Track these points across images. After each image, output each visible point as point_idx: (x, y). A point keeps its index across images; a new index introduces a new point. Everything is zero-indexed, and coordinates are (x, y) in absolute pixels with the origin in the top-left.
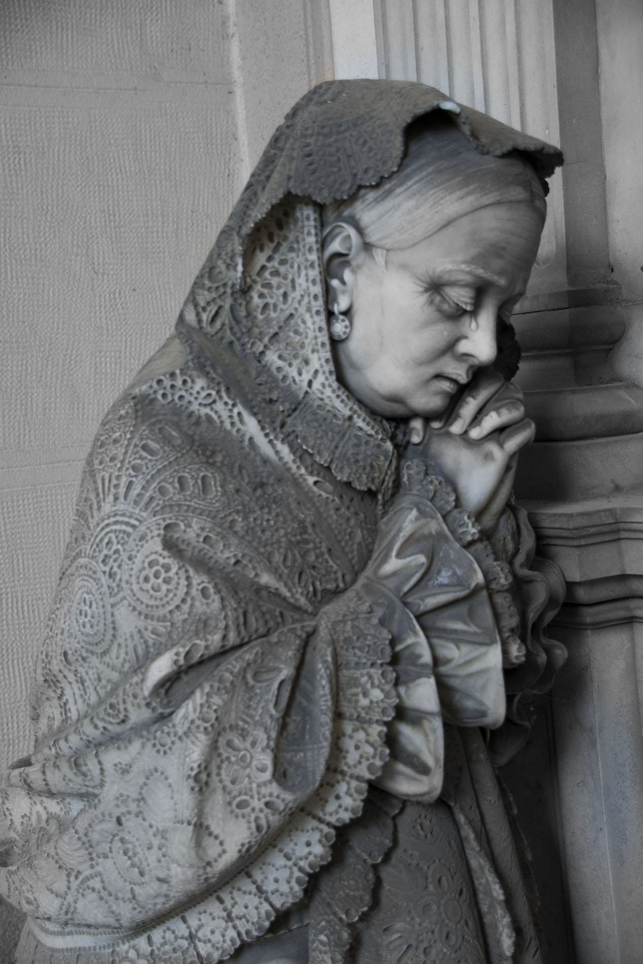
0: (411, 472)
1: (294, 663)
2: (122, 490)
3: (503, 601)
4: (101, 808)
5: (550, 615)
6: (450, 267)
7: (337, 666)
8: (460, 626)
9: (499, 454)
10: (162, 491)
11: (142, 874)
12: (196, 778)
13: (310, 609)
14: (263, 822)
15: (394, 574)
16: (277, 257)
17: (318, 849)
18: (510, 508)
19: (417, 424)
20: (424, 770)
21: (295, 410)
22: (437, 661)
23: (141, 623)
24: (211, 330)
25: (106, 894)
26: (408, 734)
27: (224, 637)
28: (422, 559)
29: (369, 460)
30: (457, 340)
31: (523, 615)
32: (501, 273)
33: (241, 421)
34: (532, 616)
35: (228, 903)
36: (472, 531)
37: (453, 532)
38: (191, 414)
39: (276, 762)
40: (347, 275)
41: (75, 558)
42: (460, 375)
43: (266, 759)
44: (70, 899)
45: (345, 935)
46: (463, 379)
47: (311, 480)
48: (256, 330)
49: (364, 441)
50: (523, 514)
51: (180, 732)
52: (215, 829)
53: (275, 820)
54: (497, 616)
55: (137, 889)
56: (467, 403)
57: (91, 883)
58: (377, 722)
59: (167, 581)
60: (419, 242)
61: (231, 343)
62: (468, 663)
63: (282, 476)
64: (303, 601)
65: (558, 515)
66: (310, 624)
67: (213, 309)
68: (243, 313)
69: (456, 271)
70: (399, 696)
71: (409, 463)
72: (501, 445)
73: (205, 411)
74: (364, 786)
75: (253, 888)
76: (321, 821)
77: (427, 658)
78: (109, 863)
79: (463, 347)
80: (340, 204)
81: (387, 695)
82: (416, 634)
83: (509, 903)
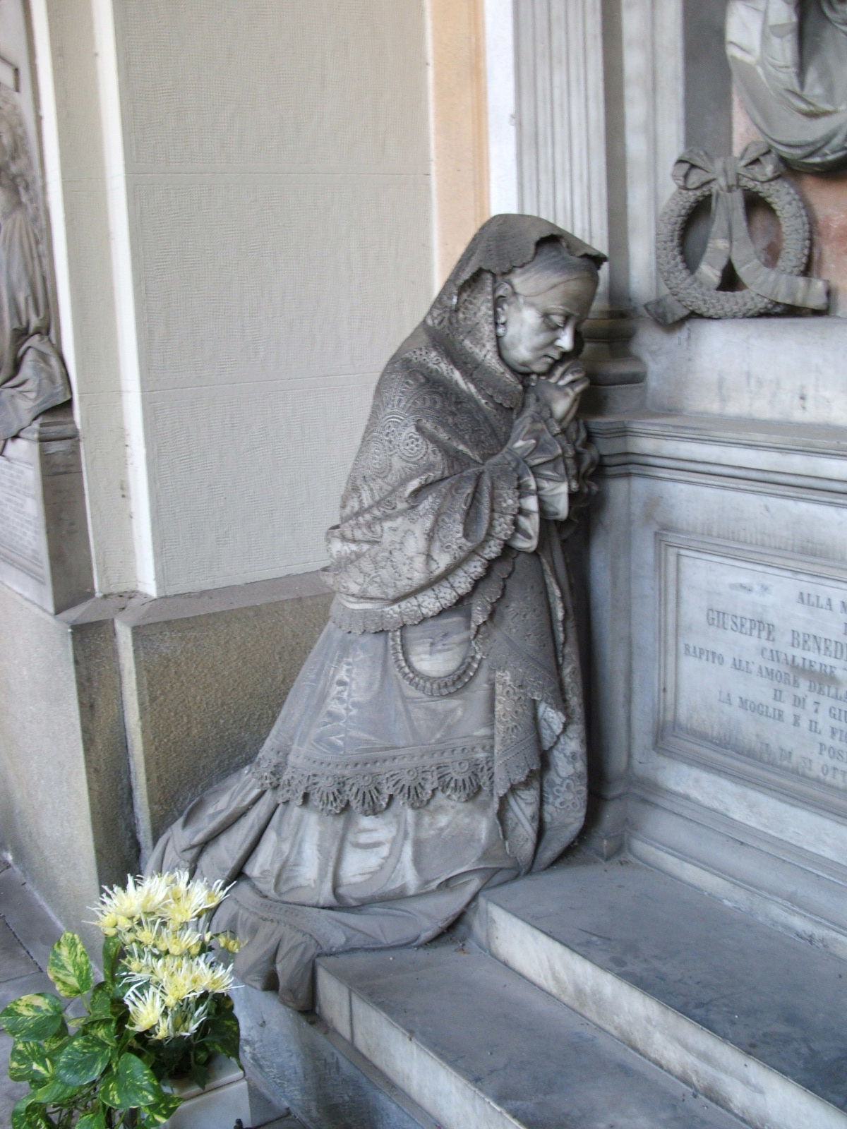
1: (474, 485)
2: (396, 402)
3: (570, 462)
4: (383, 546)
5: (592, 470)
7: (493, 487)
8: (550, 473)
9: (572, 393)
10: (414, 403)
11: (400, 576)
12: (428, 535)
13: (481, 462)
14: (457, 555)
15: (521, 447)
16: (473, 295)
17: (480, 570)
18: (576, 419)
19: (534, 377)
20: (529, 537)
21: (476, 368)
22: (539, 488)
23: (404, 464)
24: (438, 328)
25: (382, 584)
26: (523, 521)
27: (443, 473)
28: (533, 441)
31: (578, 469)
33: (452, 372)
34: (583, 470)
35: (437, 591)
36: (557, 429)
37: (548, 428)
38: (428, 368)
39: (465, 530)
40: (505, 307)
41: (371, 432)
43: (460, 528)
44: (365, 586)
45: (489, 608)
47: (483, 401)
48: (460, 329)
50: (581, 421)
51: (422, 514)
52: (435, 557)
53: (462, 554)
54: (566, 469)
55: (398, 583)
57: (375, 579)
58: (510, 514)
59: (417, 446)
61: (448, 334)
62: (553, 490)
63: (470, 398)
64: (478, 458)
65: (598, 422)
66: (481, 468)
67: (440, 318)
68: (455, 321)
70: (520, 503)
72: (573, 389)
73: (436, 366)
74: (502, 542)
75: (448, 585)
76: (482, 557)
77: (533, 487)
78: (384, 571)
79: (559, 343)
80: (504, 274)
81: (515, 503)
82: (529, 475)
83: (562, 598)
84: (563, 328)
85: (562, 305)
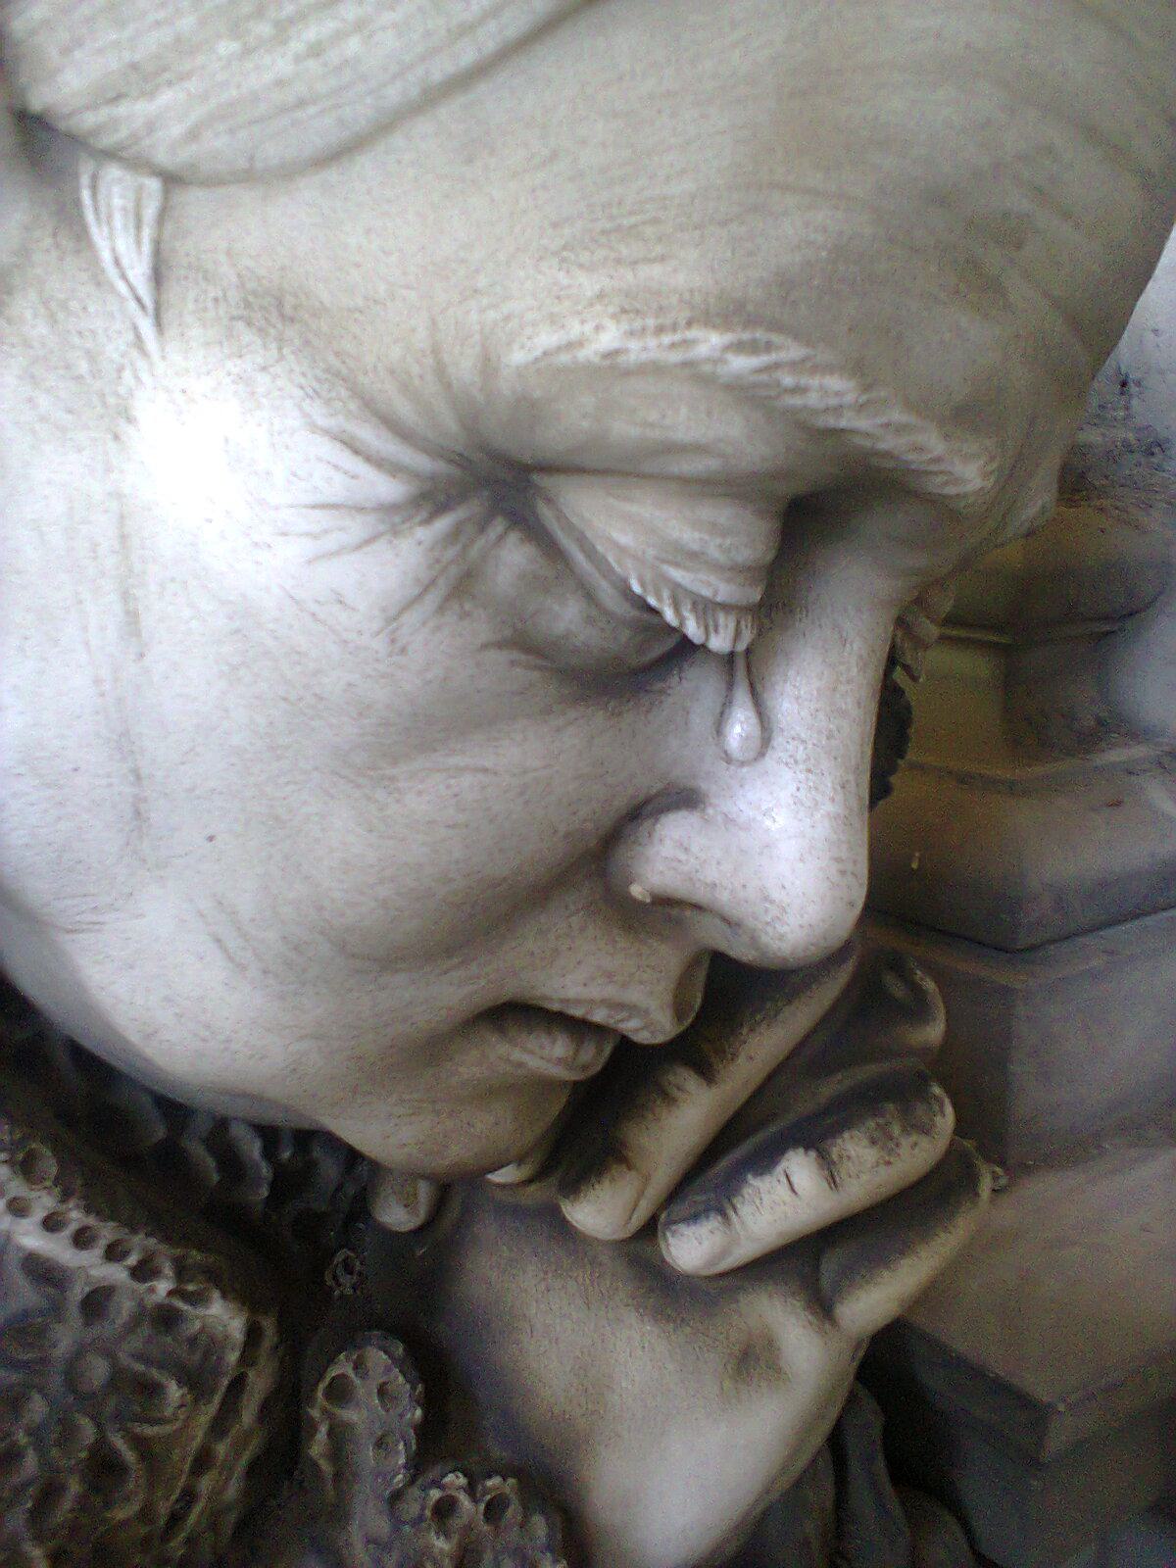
0: (350, 1414)
6: (609, 337)
9: (808, 1352)
29: (88, 1430)
30: (638, 814)
32: (966, 416)
42: (632, 1009)
46: (651, 1018)
49: (77, 1292)
56: (670, 1100)
60: (386, 125)
69: (653, 369)
71: (343, 1367)
72: (823, 1307)
84: (747, 670)
85: (728, 312)
